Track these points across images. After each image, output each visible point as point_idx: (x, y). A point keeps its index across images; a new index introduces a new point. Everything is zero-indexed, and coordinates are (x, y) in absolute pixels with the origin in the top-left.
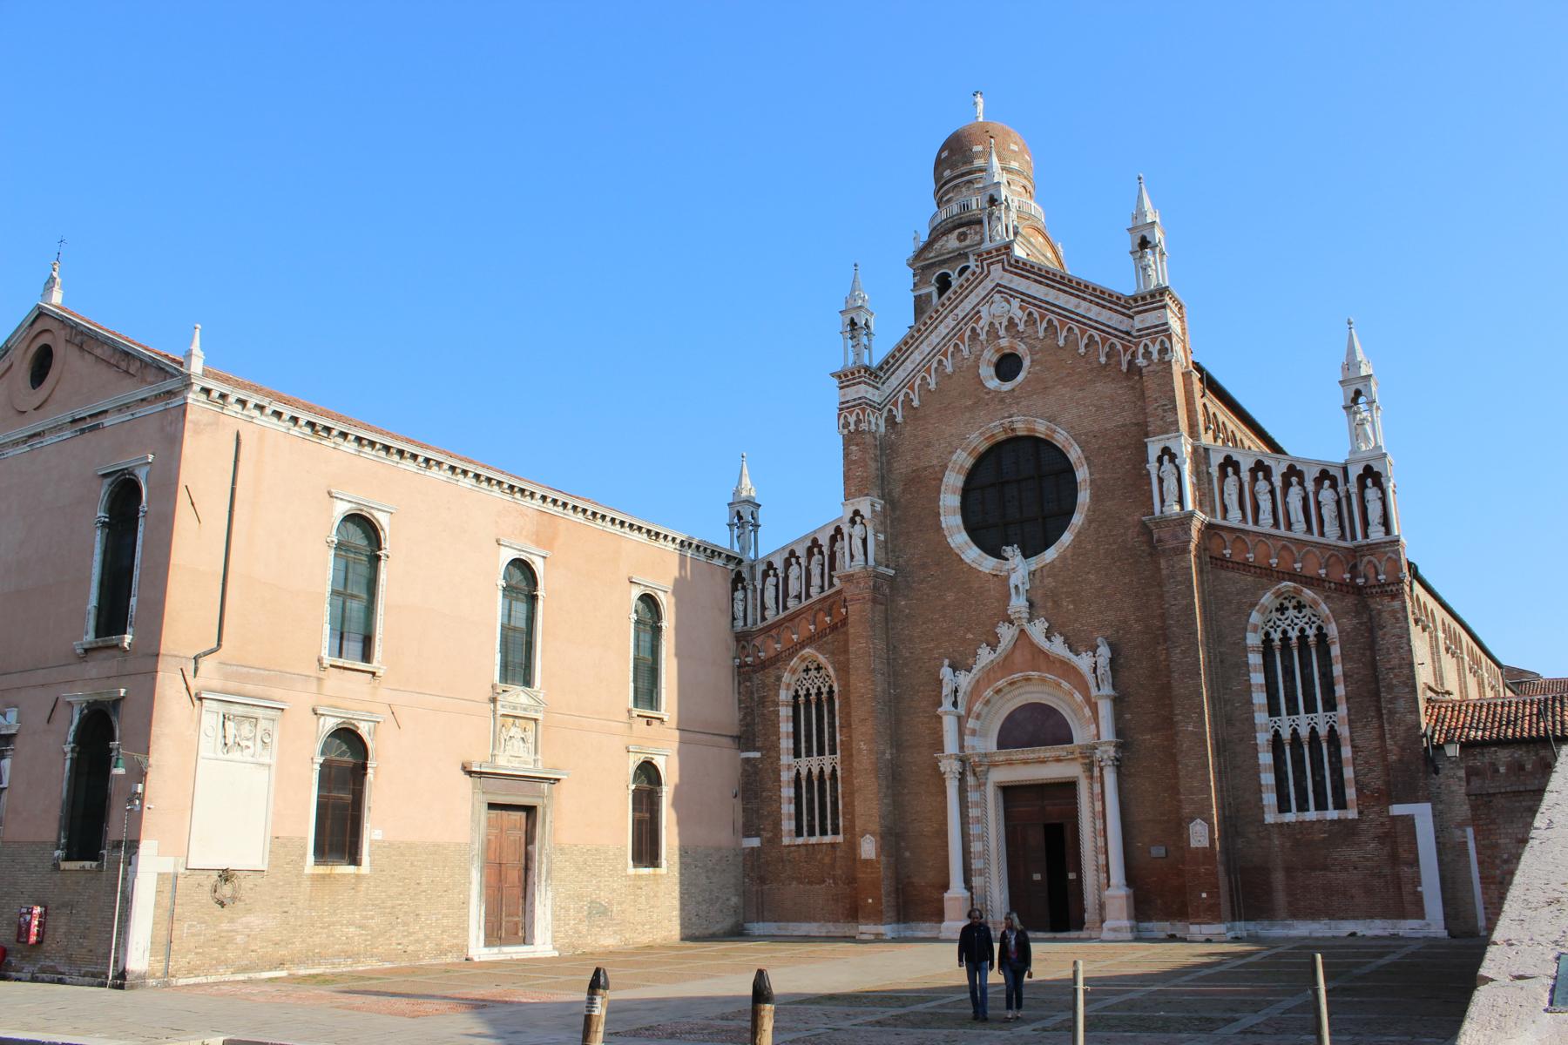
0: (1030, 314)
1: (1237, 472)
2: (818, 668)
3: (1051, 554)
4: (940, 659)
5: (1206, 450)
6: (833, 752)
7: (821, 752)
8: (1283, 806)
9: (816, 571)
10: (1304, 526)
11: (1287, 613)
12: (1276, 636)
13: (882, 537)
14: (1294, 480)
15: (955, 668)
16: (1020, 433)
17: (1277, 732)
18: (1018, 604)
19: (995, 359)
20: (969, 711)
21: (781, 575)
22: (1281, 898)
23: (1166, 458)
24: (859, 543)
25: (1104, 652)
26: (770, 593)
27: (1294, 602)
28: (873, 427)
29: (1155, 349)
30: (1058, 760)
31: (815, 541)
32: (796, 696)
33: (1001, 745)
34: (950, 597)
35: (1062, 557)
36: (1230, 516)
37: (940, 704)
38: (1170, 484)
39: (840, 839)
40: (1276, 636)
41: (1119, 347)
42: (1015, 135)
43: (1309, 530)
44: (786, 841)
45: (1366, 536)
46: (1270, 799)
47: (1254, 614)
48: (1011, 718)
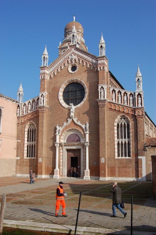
0: (79, 59)
1: (115, 92)
2: (33, 125)
3: (79, 105)
5: (110, 88)
6: (35, 141)
7: (32, 141)
8: (119, 156)
9: (34, 106)
12: (120, 124)
13: (47, 100)
14: (125, 95)
15: (59, 126)
16: (75, 82)
17: (118, 142)
19: (71, 67)
20: (61, 134)
21: (27, 106)
22: (117, 173)
24: (43, 101)
25: (88, 125)
26: (25, 109)
27: (123, 118)
28: (47, 78)
29: (102, 67)
31: (34, 100)
32: (28, 130)
33: (67, 141)
34: (59, 112)
35: (81, 106)
36: (113, 100)
38: (102, 93)
39: (35, 158)
40: (120, 124)
41: (95, 66)
42: (81, 25)
43: (127, 104)
44: (25, 158)
45: (138, 106)
46: (116, 154)
47: (116, 119)
48: (69, 136)
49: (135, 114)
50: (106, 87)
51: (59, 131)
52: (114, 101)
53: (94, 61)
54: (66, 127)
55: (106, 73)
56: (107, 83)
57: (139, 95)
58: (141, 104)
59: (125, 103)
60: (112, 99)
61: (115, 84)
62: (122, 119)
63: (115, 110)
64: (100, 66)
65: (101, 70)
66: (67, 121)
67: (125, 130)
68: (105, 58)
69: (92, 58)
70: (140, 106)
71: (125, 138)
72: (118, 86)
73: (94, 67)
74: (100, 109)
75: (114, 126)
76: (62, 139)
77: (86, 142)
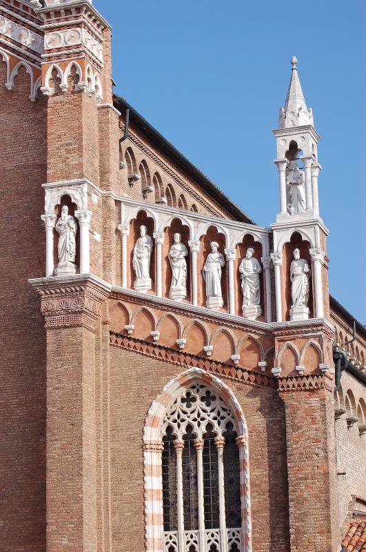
1: (150, 231)
5: (118, 203)
10: (221, 302)
11: (194, 405)
12: (180, 432)
14: (215, 245)
23: (66, 208)
27: (203, 392)
29: (65, 75)
36: (138, 283)
38: (68, 238)
40: (180, 432)
41: (29, 71)
43: (226, 305)
45: (288, 317)
47: (154, 403)
49: (270, 365)
50: (95, 199)
52: (143, 286)
53: (27, 39)
55: (96, 113)
56: (104, 173)
57: (298, 243)
58: (311, 303)
59: (211, 301)
60: (134, 276)
61: (167, 179)
62: (194, 400)
63: (149, 342)
64: (55, 70)
65: (59, 91)
67: (210, 470)
68: (84, 18)
69: (10, 17)
70: (301, 315)
71: (212, 522)
72: (195, 196)
73: (22, 77)
74: (50, 337)
75: (143, 447)
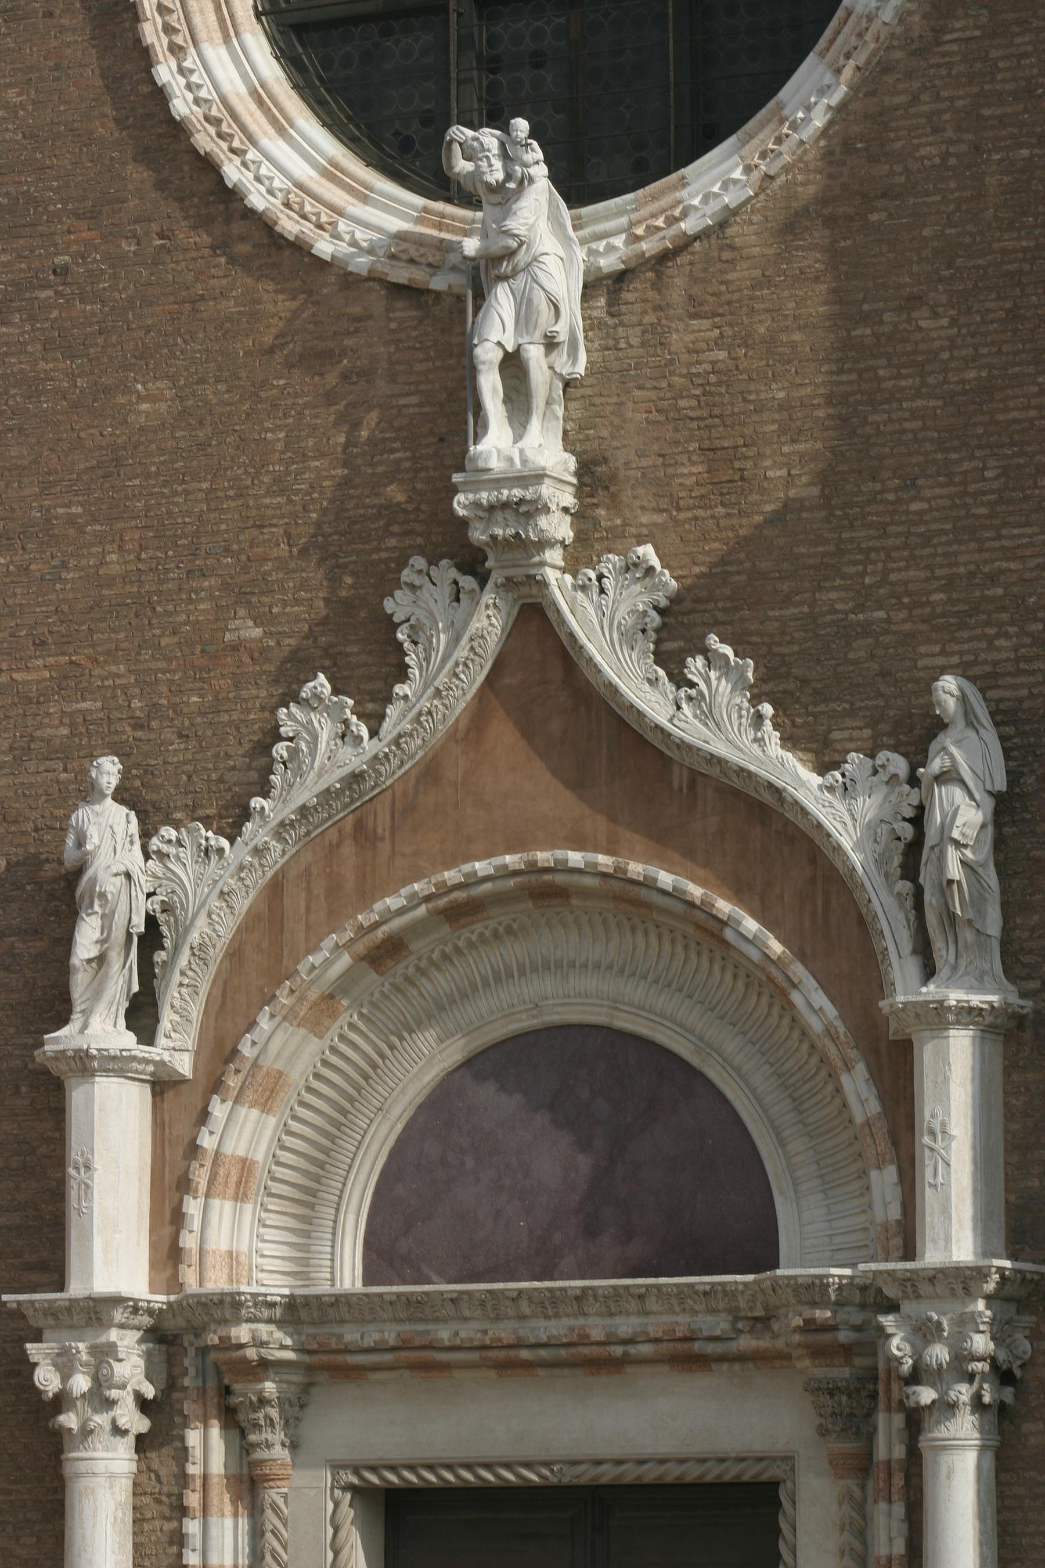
3: (716, 183)
4: (76, 756)
18: (523, 448)
20: (220, 1054)
30: (686, 1357)
33: (381, 1256)
34: (149, 401)
37: (59, 1010)
51: (151, 938)
54: (362, 827)
66: (371, 667)
76: (241, 1181)
77: (911, 1284)
